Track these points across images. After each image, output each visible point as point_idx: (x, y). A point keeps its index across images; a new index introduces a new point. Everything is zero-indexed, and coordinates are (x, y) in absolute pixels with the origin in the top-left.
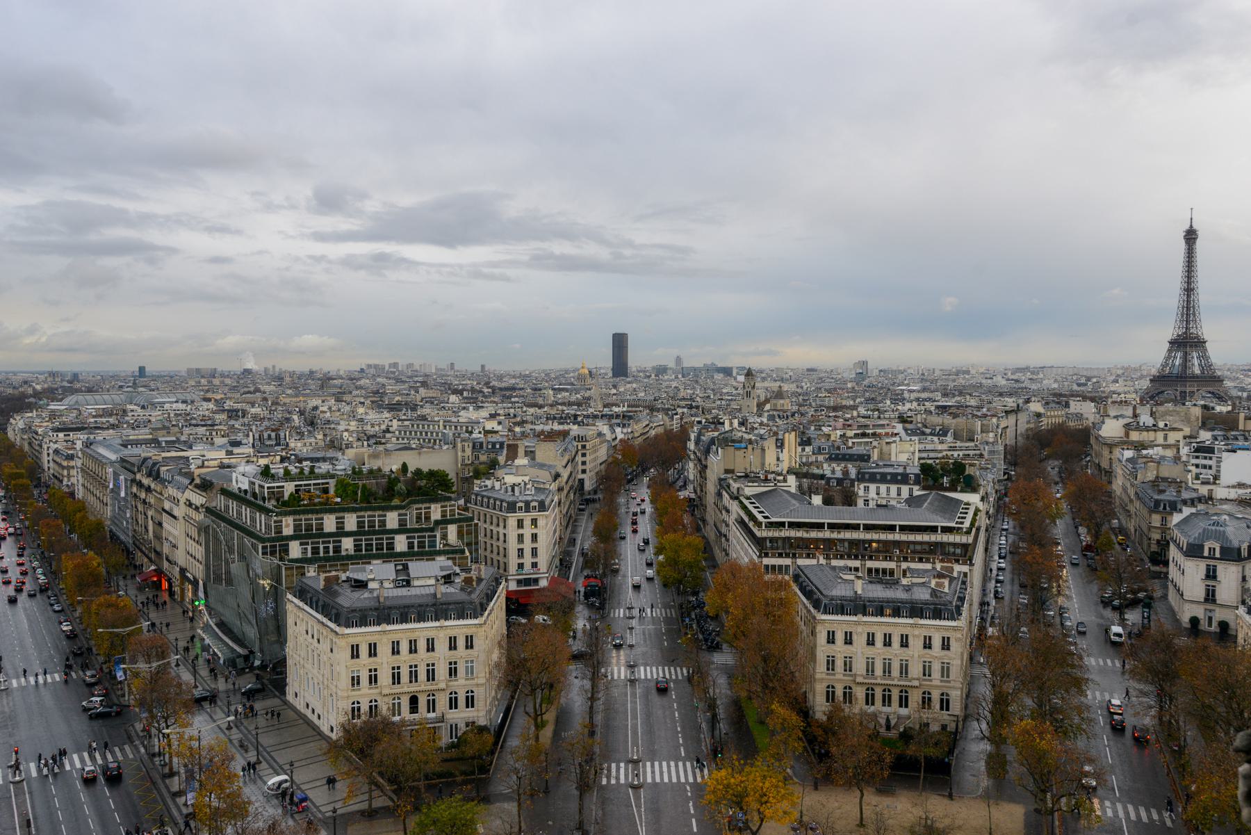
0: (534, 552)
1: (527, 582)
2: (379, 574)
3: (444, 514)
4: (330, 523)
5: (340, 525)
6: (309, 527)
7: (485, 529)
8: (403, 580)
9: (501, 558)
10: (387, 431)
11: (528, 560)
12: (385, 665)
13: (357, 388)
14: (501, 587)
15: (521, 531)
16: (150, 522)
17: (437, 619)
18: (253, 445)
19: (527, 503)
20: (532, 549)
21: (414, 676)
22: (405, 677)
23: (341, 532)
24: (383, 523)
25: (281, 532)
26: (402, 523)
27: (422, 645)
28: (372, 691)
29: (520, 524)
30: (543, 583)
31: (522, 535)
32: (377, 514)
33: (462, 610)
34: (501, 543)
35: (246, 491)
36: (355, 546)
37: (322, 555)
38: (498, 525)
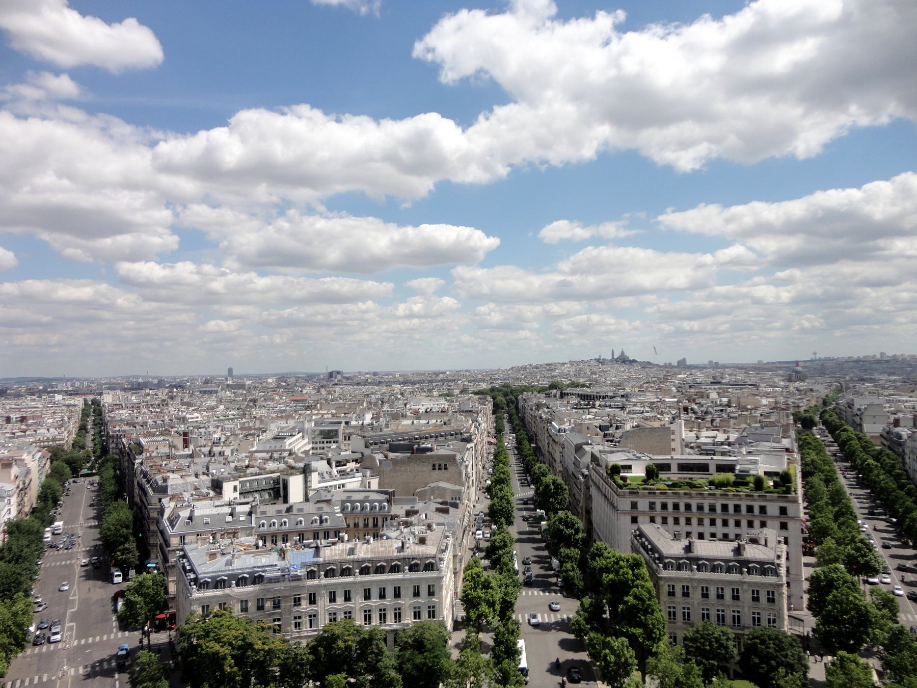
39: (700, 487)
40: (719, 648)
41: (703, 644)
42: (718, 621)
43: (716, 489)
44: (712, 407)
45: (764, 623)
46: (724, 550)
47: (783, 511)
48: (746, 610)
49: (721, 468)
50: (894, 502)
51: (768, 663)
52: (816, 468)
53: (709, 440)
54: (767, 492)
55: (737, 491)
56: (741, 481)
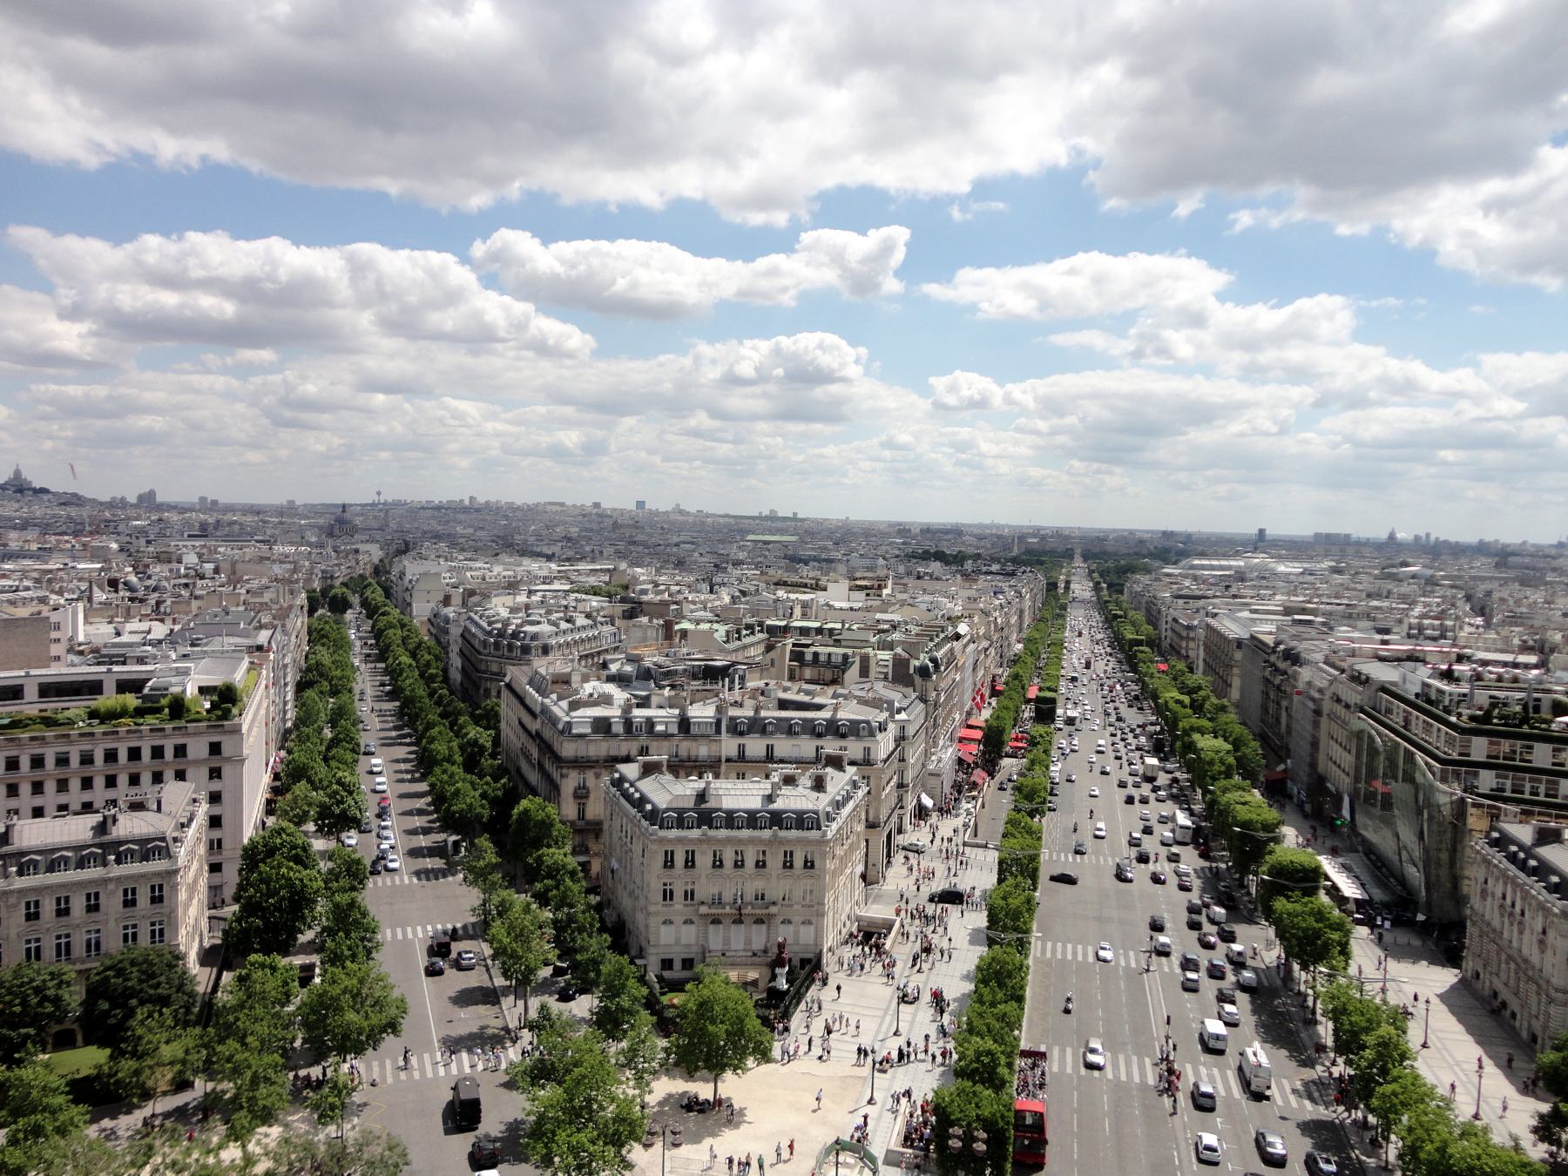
13: (1554, 570)
16: (1284, 714)
25: (1468, 755)
39: (71, 723)
40: (40, 1004)
41: (10, 1004)
42: (59, 954)
43: (102, 723)
44: (167, 579)
45: (144, 940)
46: (79, 829)
47: (215, 749)
48: (112, 923)
49: (124, 686)
50: (417, 716)
51: (124, 1005)
52: (321, 675)
53: (137, 638)
54: (187, 722)
55: (136, 724)
56: (149, 708)
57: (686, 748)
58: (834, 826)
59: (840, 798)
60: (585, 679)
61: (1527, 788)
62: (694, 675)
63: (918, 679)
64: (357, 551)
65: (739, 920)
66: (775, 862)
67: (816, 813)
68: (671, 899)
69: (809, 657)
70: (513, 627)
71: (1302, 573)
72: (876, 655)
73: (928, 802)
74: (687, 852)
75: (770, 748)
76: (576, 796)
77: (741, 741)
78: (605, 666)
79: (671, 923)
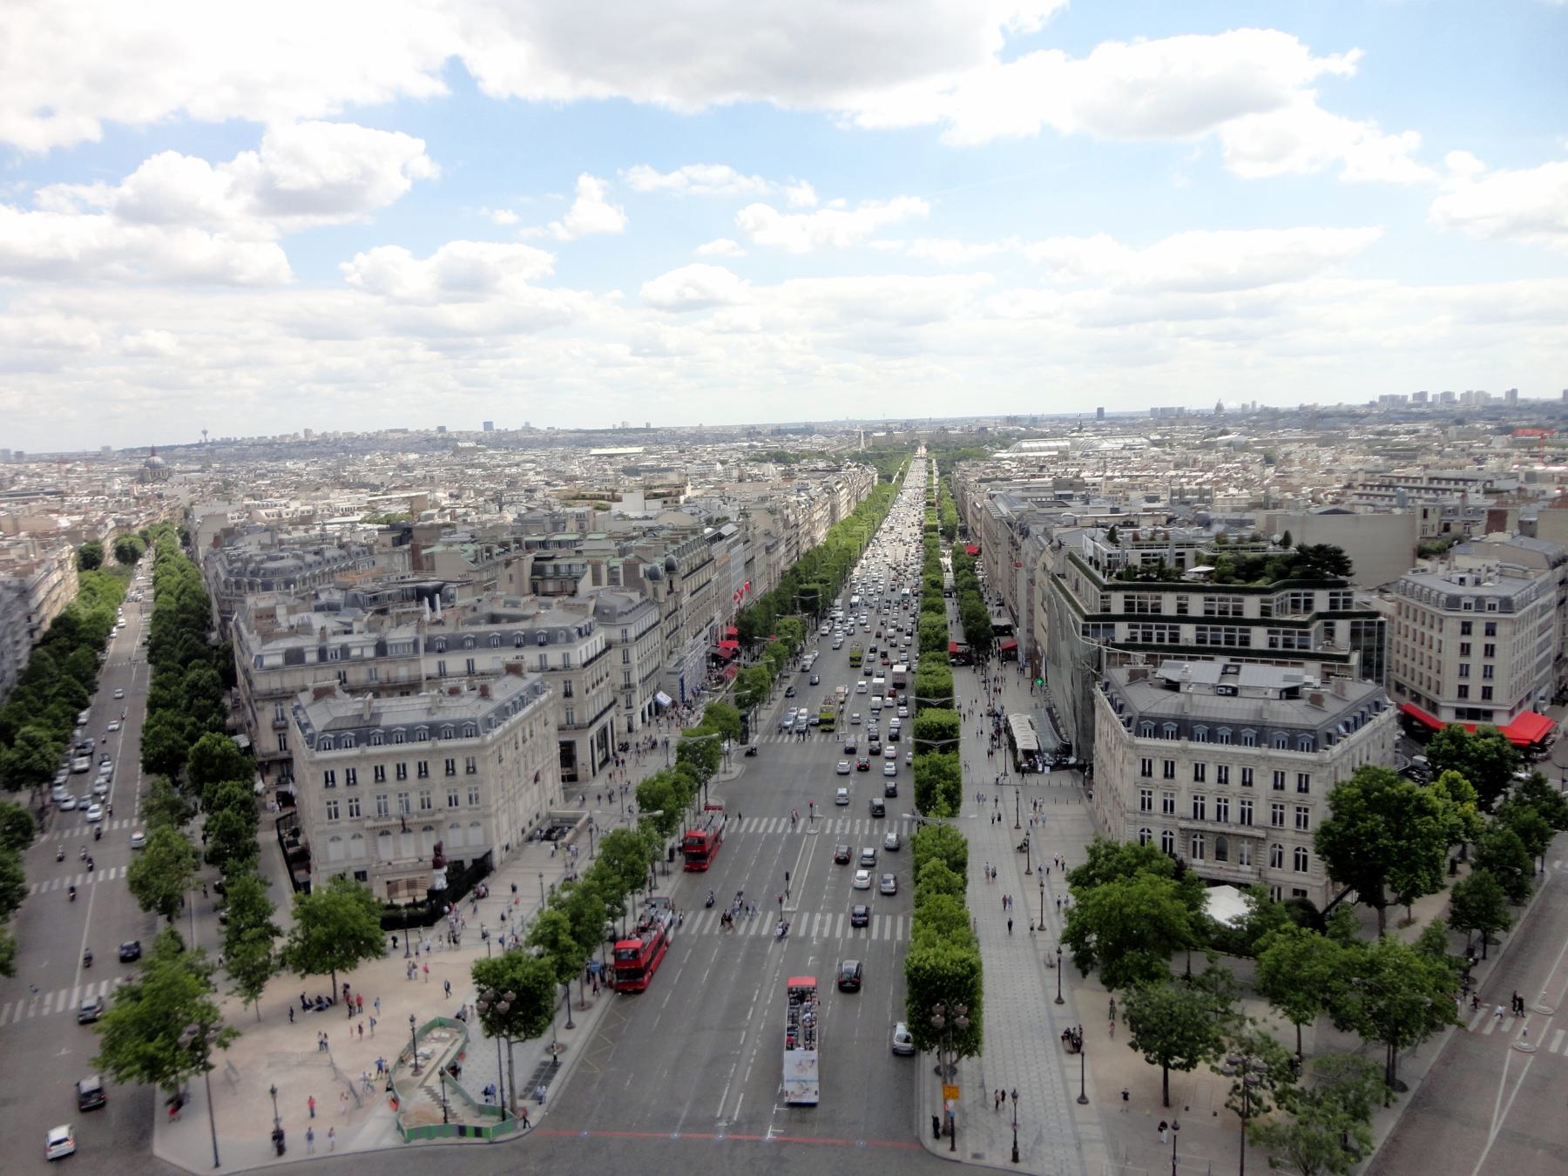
0: (1488, 672)
1: (1474, 714)
2: (1206, 671)
3: (1333, 604)
4: (1169, 604)
5: (1182, 608)
6: (1143, 608)
7: (1407, 627)
8: (1227, 687)
9: (1432, 674)
10: (1349, 486)
11: (1476, 684)
12: (1184, 792)
14: (1384, 716)
15: (1466, 639)
17: (1258, 745)
18: (1171, 500)
19: (1480, 601)
20: (1486, 667)
21: (1222, 813)
22: (1210, 812)
23: (1182, 616)
24: (1238, 611)
25: (1108, 610)
26: (1265, 611)
27: (1235, 775)
28: (1167, 821)
29: (1466, 628)
30: (1501, 720)
31: (1468, 645)
32: (1231, 596)
33: (1294, 739)
34: (1433, 653)
35: (1091, 559)
36: (1198, 636)
37: (1155, 642)
38: (1432, 627)
57: (384, 671)
58: (498, 731)
59: (509, 704)
60: (292, 610)
61: (1155, 637)
62: (405, 597)
63: (648, 583)
64: (160, 496)
65: (405, 829)
66: (437, 770)
67: (473, 720)
68: (336, 816)
69: (550, 570)
70: (253, 565)
71: (1123, 449)
72: (608, 563)
73: (664, 699)
74: (348, 771)
75: (470, 663)
76: (275, 728)
77: (441, 658)
78: (316, 596)
79: (339, 839)
